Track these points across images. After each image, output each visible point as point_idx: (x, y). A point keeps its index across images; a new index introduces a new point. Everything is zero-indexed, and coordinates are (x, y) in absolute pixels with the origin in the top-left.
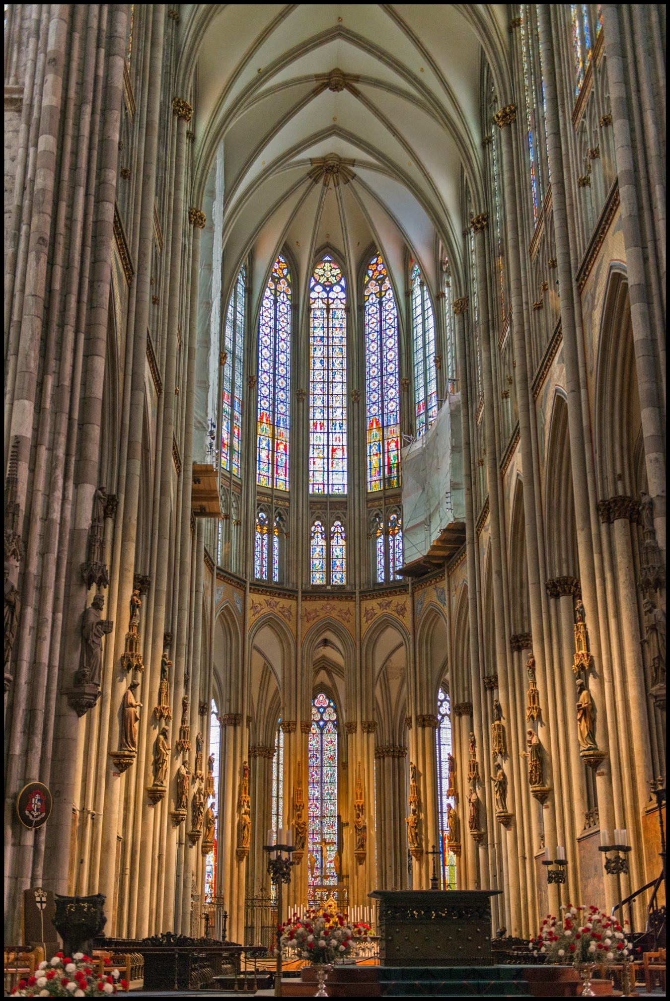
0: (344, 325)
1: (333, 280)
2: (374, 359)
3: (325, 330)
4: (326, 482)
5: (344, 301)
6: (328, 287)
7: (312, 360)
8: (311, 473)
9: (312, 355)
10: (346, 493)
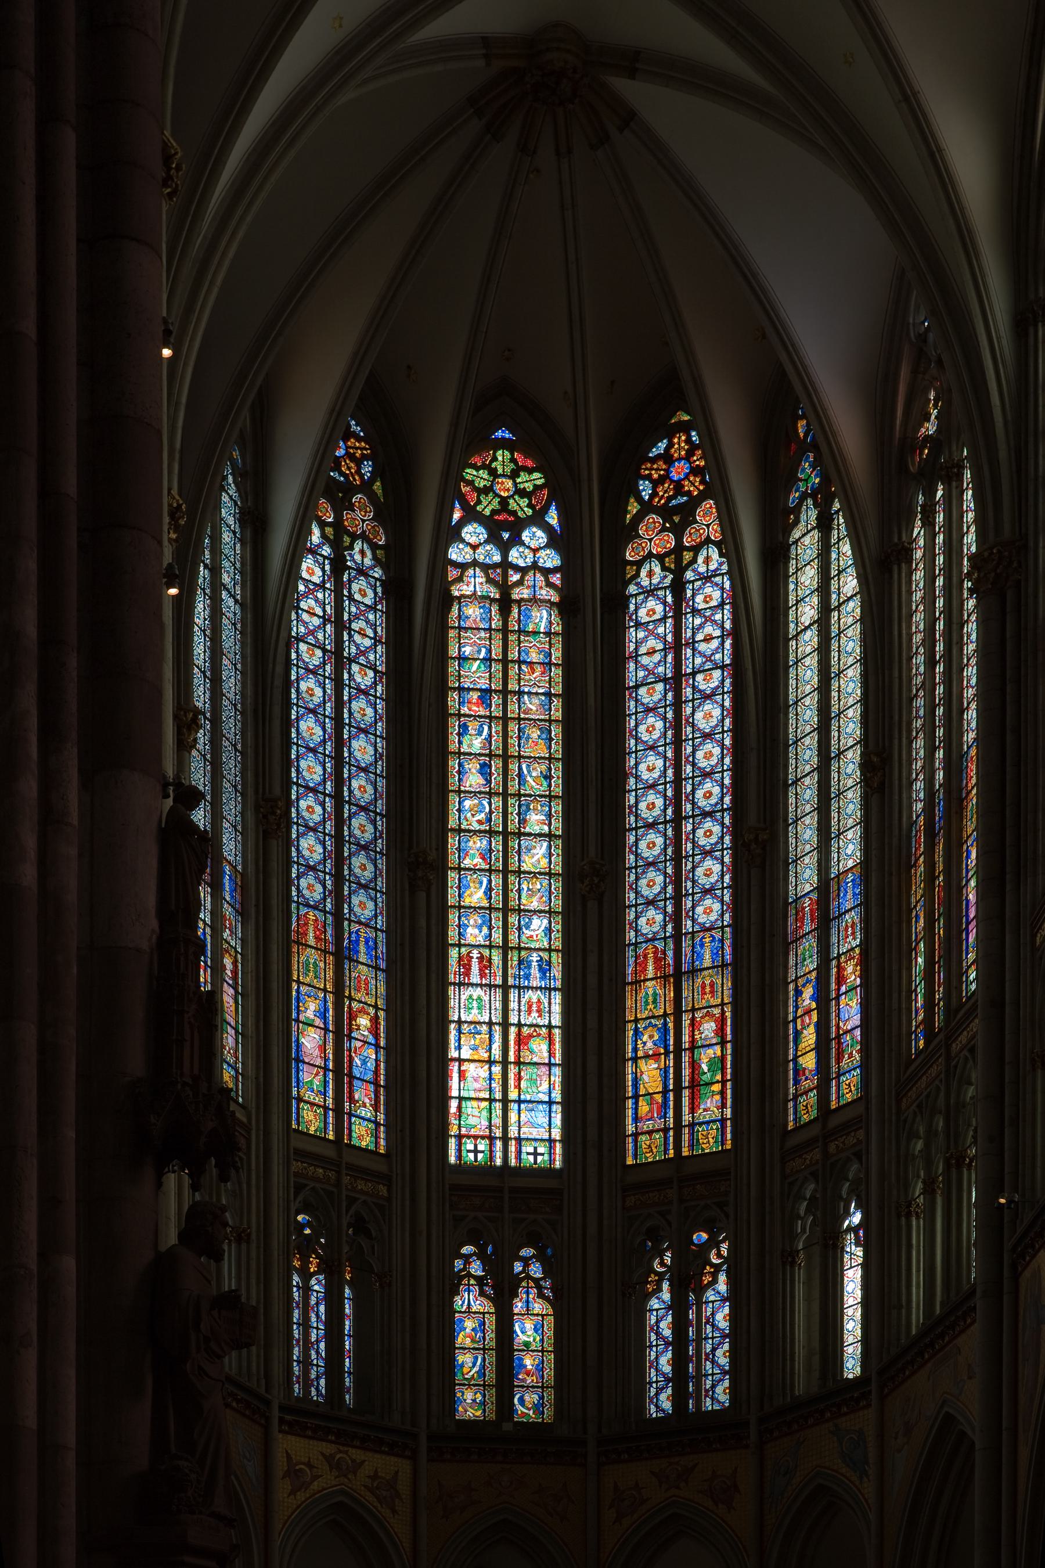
0: (557, 655)
1: (521, 507)
2: (650, 767)
3: (497, 667)
4: (498, 1133)
7: (453, 764)
8: (454, 1105)
9: (453, 747)
10: (558, 1164)
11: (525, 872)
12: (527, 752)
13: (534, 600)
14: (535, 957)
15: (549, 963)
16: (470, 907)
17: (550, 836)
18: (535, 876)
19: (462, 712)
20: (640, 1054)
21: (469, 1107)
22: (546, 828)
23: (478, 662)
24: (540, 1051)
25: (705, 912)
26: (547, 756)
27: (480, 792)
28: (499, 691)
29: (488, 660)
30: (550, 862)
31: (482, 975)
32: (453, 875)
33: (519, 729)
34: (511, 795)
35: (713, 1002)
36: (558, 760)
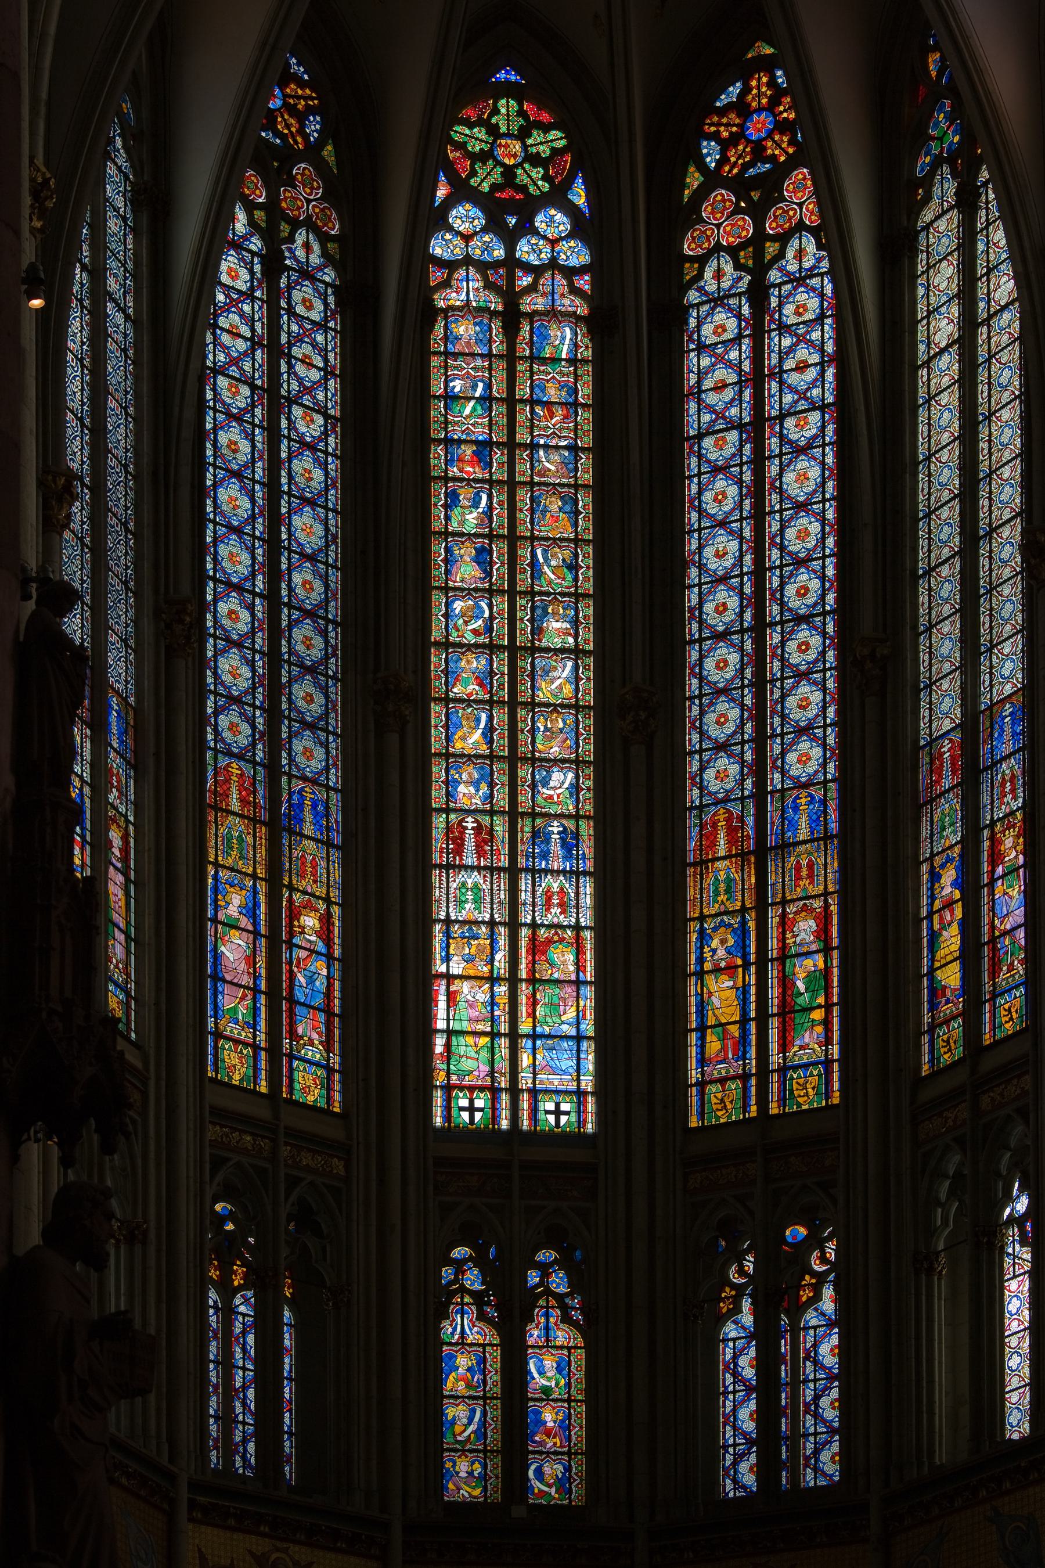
5: (584, 282)
11: (542, 704)
12: (543, 531)
13: (553, 314)
14: (555, 828)
15: (576, 835)
16: (462, 755)
17: (576, 652)
18: (555, 710)
19: (450, 474)
21: (463, 1046)
22: (571, 640)
23: (472, 403)
24: (564, 963)
25: (799, 761)
26: (572, 536)
27: (476, 590)
28: (502, 444)
29: (487, 400)
30: (577, 690)
32: (438, 709)
33: (532, 499)
34: (520, 593)
35: (812, 890)
36: (587, 542)
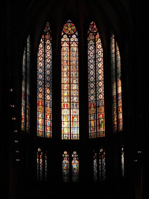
4: (69, 133)
6: (70, 36)
8: (62, 129)
15: (77, 105)
17: (77, 84)
20: (91, 120)
31: (67, 107)
